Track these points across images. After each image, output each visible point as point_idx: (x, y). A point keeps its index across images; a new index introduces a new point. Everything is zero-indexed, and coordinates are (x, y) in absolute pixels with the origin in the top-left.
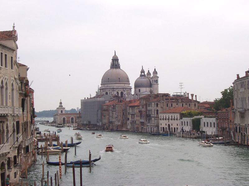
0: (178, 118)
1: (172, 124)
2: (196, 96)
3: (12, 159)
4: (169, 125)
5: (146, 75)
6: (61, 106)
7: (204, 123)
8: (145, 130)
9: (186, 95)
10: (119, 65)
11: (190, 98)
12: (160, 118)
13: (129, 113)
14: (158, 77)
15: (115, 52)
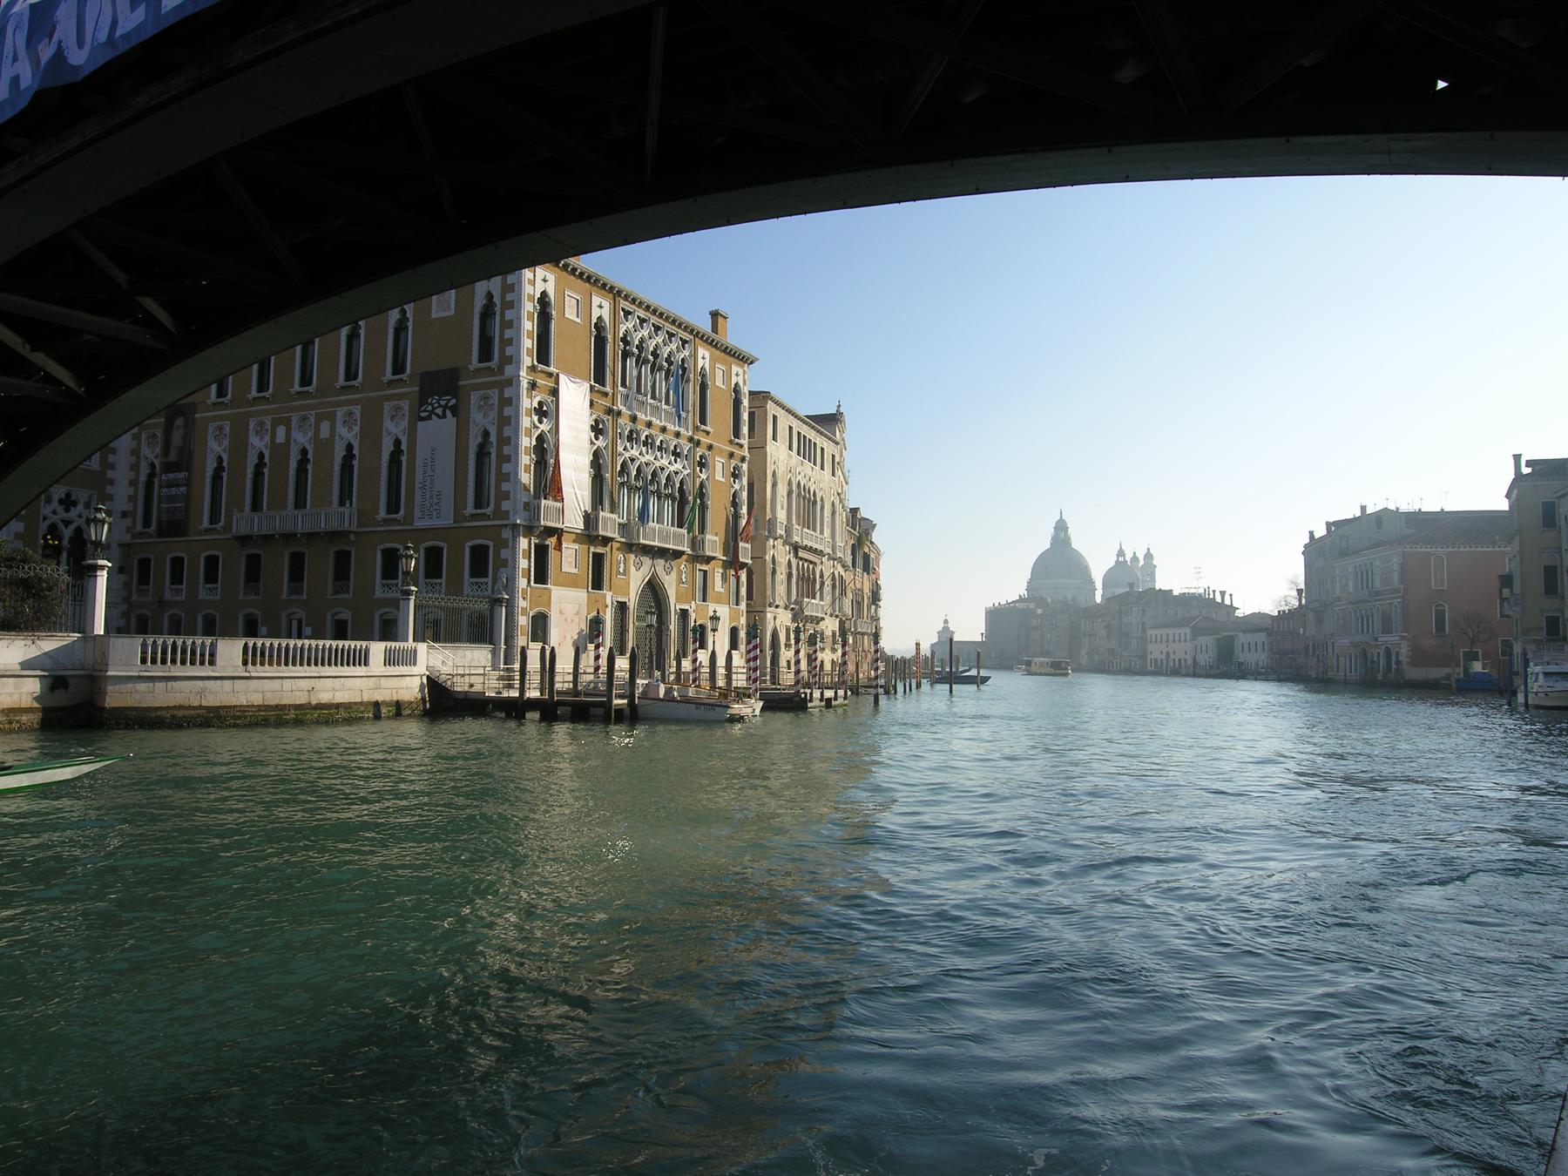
0: (1188, 639)
1: (1174, 653)
2: (1231, 595)
3: (828, 633)
4: (1168, 655)
5: (1129, 560)
6: (946, 629)
7: (1243, 644)
8: (1117, 666)
9: (1209, 594)
10: (1070, 539)
11: (1218, 599)
12: (1149, 639)
13: (1084, 632)
14: (1155, 566)
15: (1061, 513)
